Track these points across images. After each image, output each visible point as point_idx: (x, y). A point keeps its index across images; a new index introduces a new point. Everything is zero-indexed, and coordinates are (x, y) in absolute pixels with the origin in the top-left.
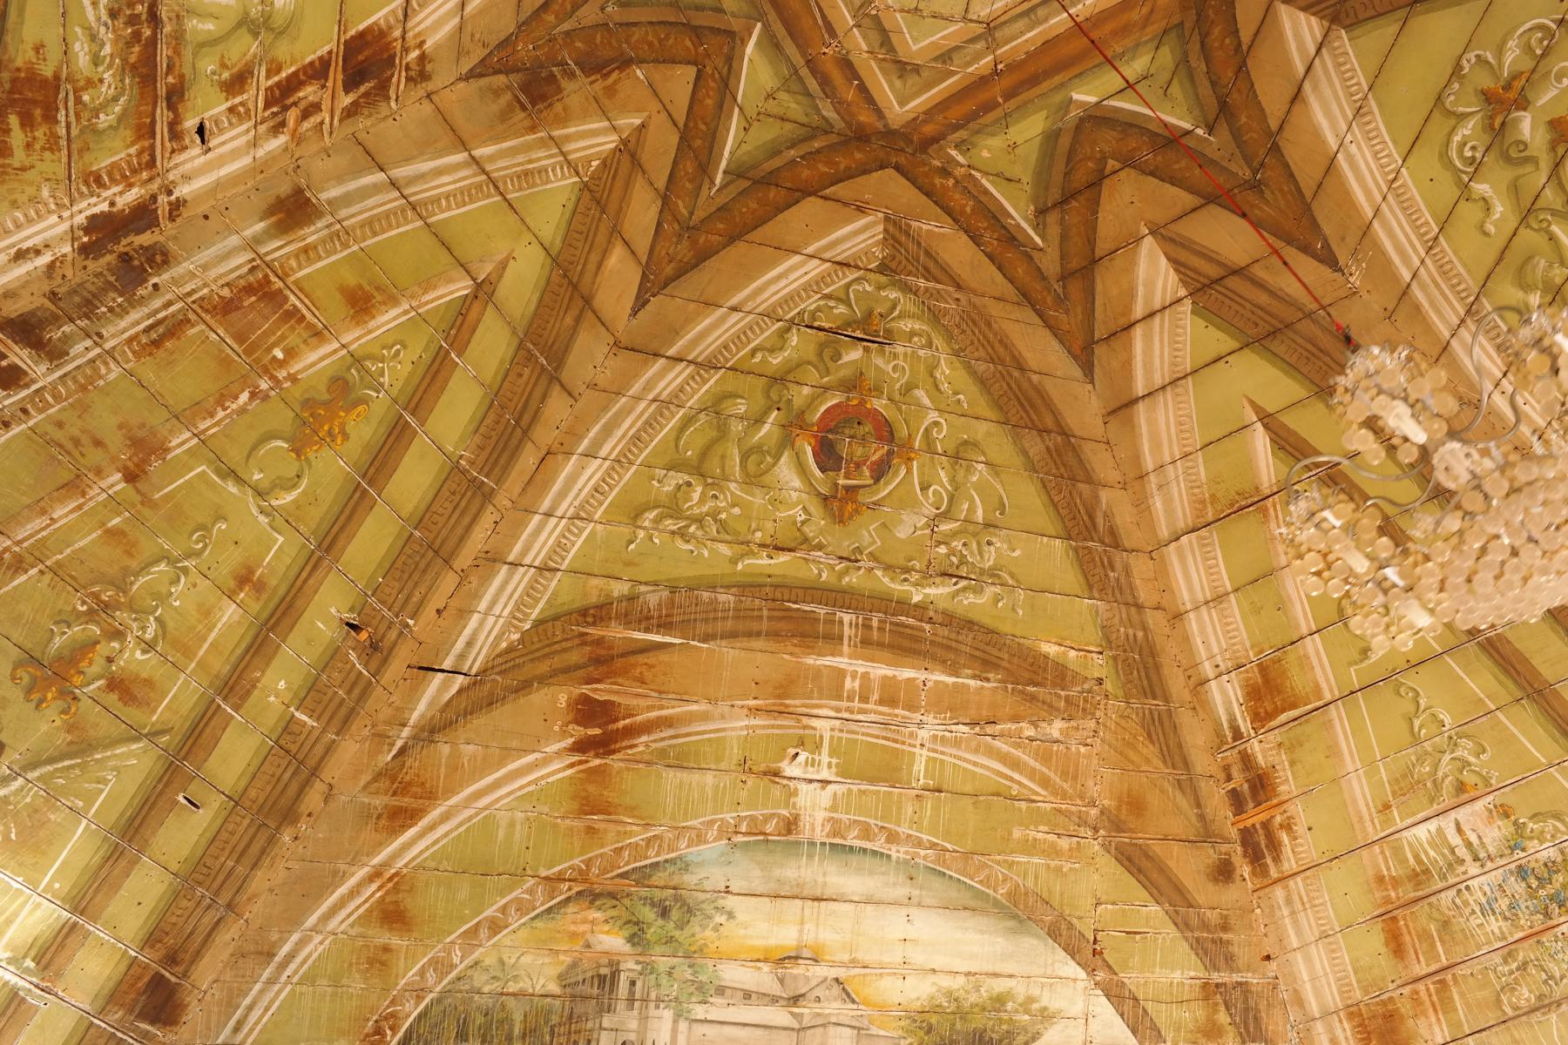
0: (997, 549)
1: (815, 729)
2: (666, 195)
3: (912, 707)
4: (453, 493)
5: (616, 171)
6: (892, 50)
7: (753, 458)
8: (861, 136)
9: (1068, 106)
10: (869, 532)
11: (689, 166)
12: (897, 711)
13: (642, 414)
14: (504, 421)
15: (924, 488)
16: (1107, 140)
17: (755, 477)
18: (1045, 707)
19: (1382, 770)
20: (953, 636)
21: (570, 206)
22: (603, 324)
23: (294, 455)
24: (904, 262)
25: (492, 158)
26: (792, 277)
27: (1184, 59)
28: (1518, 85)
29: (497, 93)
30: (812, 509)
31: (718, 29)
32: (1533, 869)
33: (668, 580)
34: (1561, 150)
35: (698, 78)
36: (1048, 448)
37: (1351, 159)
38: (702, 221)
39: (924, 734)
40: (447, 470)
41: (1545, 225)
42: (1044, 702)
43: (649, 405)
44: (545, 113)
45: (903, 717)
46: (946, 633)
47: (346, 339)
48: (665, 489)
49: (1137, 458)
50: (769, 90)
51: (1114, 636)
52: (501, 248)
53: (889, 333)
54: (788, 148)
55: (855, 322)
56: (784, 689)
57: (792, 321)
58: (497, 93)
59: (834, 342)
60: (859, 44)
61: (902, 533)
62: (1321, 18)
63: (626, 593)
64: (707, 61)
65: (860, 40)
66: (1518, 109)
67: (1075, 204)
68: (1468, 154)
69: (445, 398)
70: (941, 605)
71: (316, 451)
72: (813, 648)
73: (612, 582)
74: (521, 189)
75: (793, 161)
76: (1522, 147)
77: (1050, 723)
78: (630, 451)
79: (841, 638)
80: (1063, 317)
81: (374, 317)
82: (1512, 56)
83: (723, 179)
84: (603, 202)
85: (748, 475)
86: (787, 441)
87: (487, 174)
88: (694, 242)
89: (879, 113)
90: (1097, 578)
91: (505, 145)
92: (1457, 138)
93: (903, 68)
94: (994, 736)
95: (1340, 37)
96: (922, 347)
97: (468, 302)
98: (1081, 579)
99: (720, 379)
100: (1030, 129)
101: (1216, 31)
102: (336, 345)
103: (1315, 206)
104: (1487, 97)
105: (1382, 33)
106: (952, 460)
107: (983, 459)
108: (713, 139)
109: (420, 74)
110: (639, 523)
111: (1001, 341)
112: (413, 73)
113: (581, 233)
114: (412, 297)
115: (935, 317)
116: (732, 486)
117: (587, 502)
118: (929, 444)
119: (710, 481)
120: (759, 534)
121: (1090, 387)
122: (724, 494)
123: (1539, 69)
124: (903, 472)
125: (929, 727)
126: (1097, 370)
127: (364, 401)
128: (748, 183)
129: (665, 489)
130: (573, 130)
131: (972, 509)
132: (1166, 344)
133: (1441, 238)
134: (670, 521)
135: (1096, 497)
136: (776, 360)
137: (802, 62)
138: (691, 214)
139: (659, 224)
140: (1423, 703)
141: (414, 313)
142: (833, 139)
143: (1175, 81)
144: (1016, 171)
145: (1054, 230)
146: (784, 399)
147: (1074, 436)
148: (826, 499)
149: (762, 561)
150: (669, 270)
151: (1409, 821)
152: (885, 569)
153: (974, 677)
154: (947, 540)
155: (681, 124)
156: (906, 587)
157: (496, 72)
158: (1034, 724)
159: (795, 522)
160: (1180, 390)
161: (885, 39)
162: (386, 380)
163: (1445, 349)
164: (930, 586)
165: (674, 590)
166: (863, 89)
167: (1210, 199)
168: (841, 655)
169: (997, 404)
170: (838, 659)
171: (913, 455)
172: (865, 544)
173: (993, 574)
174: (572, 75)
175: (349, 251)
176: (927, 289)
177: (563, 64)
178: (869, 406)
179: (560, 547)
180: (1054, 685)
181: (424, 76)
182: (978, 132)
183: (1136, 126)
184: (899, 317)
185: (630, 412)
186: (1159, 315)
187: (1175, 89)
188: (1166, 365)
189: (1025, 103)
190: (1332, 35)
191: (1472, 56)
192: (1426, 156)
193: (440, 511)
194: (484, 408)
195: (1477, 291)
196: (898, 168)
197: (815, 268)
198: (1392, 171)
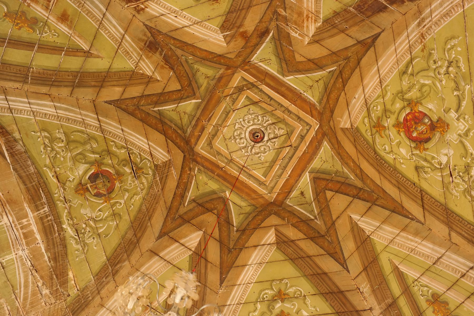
0: (93, 241)
1: (3, 218)
2: (143, 96)
3: (27, 244)
4: (20, 71)
5: (142, 78)
6: (213, 138)
7: (81, 156)
8: (187, 142)
9: (224, 192)
10: (77, 202)
11: (155, 99)
12: (23, 240)
13: (77, 117)
14: (52, 77)
15: (100, 210)
16: (220, 206)
17: (76, 159)
18: (51, 284)
20: (58, 244)
21: (126, 69)
22: (98, 94)
23: (4, 14)
24: (161, 171)
25: (127, 41)
26: (140, 142)
27: (250, 214)
28: (286, 297)
29: (145, 35)
30: (75, 181)
31: (194, 90)
33: (27, 148)
35: (179, 90)
36: (131, 239)
37: (248, 269)
38: (142, 110)
39: (20, 253)
40: (26, 65)
42: (52, 283)
43: (81, 118)
44: (147, 51)
45: (22, 243)
46: (58, 241)
47: (51, 17)
48: (57, 135)
49: (142, 265)
50: (186, 112)
51: (85, 291)
52: (103, 54)
53: (139, 177)
54: (174, 124)
55: (137, 166)
56: (11, 202)
57: (128, 148)
58: (145, 35)
59: (128, 163)
60: (210, 129)
61: (83, 211)
62: (276, 240)
63: (17, 138)
64: (184, 91)
65: (211, 129)
66: (281, 301)
67: (201, 208)
68: (265, 297)
69: (49, 55)
70: (66, 235)
71: (9, 21)
72: (30, 204)
73: (18, 132)
74: (123, 53)
75: (171, 127)
76: (273, 308)
77: (47, 289)
78: (63, 119)
79: (39, 210)
80: (170, 222)
81: (62, 24)
82: (291, 290)
83: (156, 110)
84: (132, 78)
85: (75, 157)
86: (92, 164)
87: (122, 41)
88: (135, 110)
89: (196, 144)
90: (101, 275)
91: (132, 43)
92: (267, 291)
93: (210, 144)
94: (32, 274)
95: (274, 247)
96: (140, 188)
97: (82, 51)
98: (98, 271)
99: (100, 135)
100: (213, 186)
101: (260, 217)
102: (47, 15)
103: (233, 269)
104: (280, 291)
105: (280, 256)
106: (113, 214)
107: (118, 222)
108: (165, 102)
109: (139, 11)
110: (42, 132)
111: (154, 209)
112: (137, 8)
113: (120, 76)
114: (74, 33)
115: (151, 187)
116: (69, 154)
117: (40, 113)
118: (113, 205)
119: (67, 147)
120: (58, 169)
121: (155, 241)
122: (66, 153)
123: (292, 299)
124: (101, 202)
125: (24, 253)
126: (160, 240)
127: (34, 31)
128: (159, 118)
129: (57, 135)
130: (147, 61)
131: (101, 228)
132: (177, 254)
133: (242, 305)
134: (48, 141)
135: (125, 261)
136: (114, 149)
137: (198, 117)
138: (142, 106)
139: (134, 98)
141: (70, 36)
142: (183, 135)
143: (244, 215)
144: (201, 188)
145: (191, 207)
146: (104, 157)
147: (139, 244)
148: (81, 183)
149: (50, 174)
150: (123, 106)
152: (68, 212)
153: (49, 257)
154: (88, 225)
155: (164, 91)
156: (66, 221)
157: (150, 32)
158: (43, 284)
159: (68, 178)
160: (167, 265)
161: (215, 135)
162: (44, 35)
164: (71, 228)
165: (26, 152)
166: (200, 136)
167: (220, 242)
168: (33, 213)
169: (136, 218)
170: (31, 213)
171: (108, 202)
172: (73, 202)
173: (85, 244)
174: (161, 55)
175: (78, 9)
176: (157, 181)
177: (163, 51)
178: (115, 182)
179: (21, 111)
180: (60, 283)
181: (138, 12)
182: (205, 173)
183: (228, 212)
184: (145, 177)
185: (75, 114)
186: (184, 247)
187: (242, 216)
188: (172, 257)
189: (218, 181)
190: (274, 245)
191: (287, 281)
192: (260, 287)
193: (12, 69)
194: (52, 69)
196: (185, 156)
197: (146, 147)
198: (251, 281)
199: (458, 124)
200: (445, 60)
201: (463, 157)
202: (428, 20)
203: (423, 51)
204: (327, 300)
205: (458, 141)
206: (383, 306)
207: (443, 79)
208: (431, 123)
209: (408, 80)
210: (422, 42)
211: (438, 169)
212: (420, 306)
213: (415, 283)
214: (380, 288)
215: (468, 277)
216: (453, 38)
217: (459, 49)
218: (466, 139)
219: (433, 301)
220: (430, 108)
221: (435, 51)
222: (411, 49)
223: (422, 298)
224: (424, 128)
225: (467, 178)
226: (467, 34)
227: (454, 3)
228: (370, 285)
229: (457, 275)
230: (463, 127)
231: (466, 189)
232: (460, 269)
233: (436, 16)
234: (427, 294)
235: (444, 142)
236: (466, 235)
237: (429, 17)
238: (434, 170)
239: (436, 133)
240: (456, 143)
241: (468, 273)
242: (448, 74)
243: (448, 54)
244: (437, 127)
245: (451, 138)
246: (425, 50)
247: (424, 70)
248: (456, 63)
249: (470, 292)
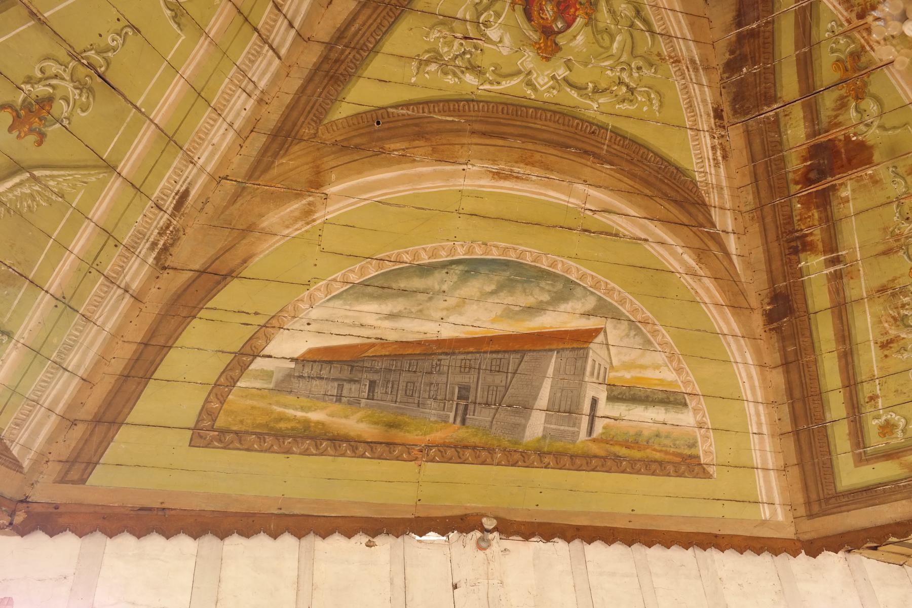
199: (547, 75)
200: (638, 85)
201: (496, 69)
202: (693, 77)
203: (659, 55)
205: (521, 67)
207: (614, 74)
208: (554, 31)
209: (626, 15)
210: (670, 57)
211: (478, 18)
215: (276, 15)
216: (661, 106)
217: (645, 109)
218: (522, 81)
220: (578, 38)
221: (653, 73)
222: (666, 37)
224: (548, 16)
225: (461, 64)
226: (659, 124)
227: (699, 119)
230: (542, 83)
231: (441, 56)
233: (694, 90)
235: (522, 43)
236: (353, 29)
237: (697, 79)
238: (476, 9)
239: (538, 34)
240: (518, 63)
241: (282, 18)
242: (619, 83)
243: (644, 91)
244: (547, 39)
245: (527, 58)
246: (658, 58)
247: (633, 48)
248: (630, 99)
249: (248, 15)
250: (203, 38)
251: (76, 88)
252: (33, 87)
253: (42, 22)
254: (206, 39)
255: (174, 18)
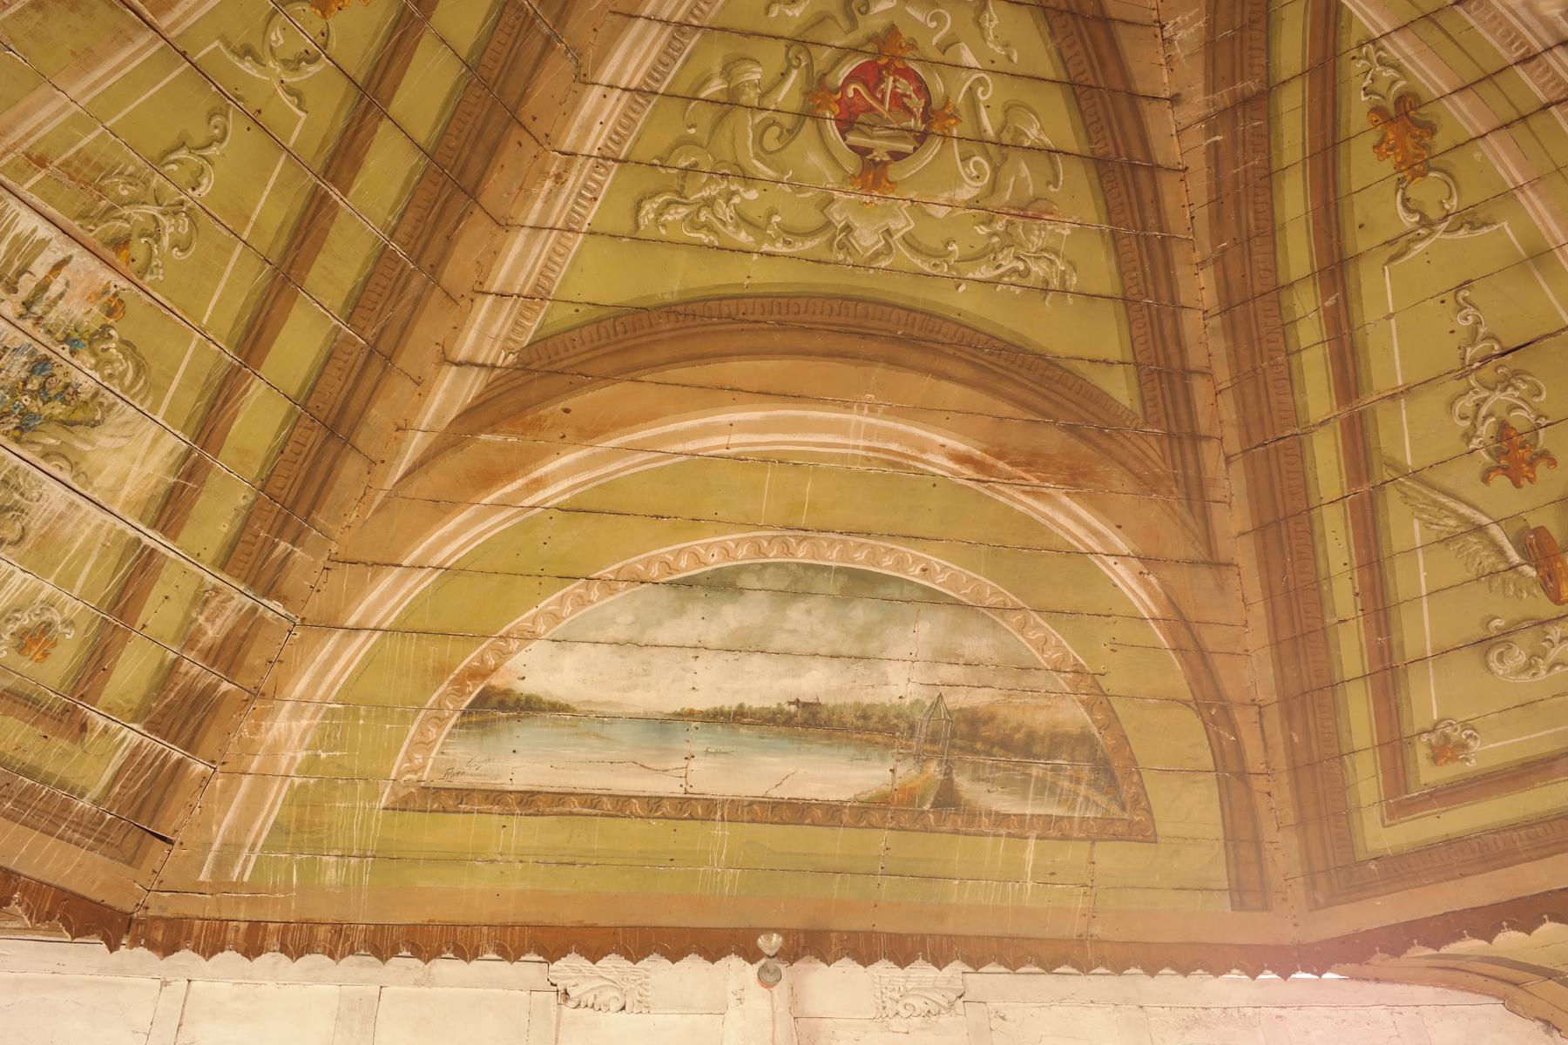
19: (92, 136)
32: (52, 375)
34: (870, 48)
41: (795, 63)
76: (863, 9)
140: (213, 151)
151: (36, 200)
163: (630, 16)
195: (706, 23)
204: (1052, 34)
206: (1224, 97)
212: (1343, 120)
213: (1364, 50)
214: (1237, 42)
215: (1540, 65)
219: (1392, 112)
223: (1363, 99)
228: (1207, 22)
229: (1511, 53)
232: (1530, 37)
234: (1384, 91)
241: (1549, 58)
249: (1518, 111)
250: (1520, 197)
251: (1505, 389)
252: (1478, 437)
253: (1407, 391)
254: (1523, 192)
255: (1473, 226)
